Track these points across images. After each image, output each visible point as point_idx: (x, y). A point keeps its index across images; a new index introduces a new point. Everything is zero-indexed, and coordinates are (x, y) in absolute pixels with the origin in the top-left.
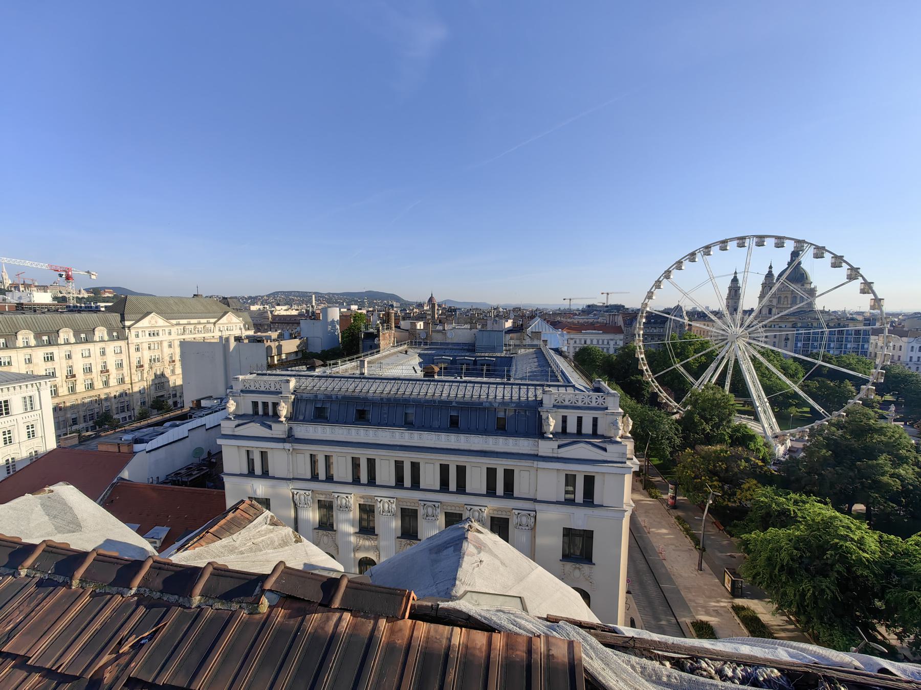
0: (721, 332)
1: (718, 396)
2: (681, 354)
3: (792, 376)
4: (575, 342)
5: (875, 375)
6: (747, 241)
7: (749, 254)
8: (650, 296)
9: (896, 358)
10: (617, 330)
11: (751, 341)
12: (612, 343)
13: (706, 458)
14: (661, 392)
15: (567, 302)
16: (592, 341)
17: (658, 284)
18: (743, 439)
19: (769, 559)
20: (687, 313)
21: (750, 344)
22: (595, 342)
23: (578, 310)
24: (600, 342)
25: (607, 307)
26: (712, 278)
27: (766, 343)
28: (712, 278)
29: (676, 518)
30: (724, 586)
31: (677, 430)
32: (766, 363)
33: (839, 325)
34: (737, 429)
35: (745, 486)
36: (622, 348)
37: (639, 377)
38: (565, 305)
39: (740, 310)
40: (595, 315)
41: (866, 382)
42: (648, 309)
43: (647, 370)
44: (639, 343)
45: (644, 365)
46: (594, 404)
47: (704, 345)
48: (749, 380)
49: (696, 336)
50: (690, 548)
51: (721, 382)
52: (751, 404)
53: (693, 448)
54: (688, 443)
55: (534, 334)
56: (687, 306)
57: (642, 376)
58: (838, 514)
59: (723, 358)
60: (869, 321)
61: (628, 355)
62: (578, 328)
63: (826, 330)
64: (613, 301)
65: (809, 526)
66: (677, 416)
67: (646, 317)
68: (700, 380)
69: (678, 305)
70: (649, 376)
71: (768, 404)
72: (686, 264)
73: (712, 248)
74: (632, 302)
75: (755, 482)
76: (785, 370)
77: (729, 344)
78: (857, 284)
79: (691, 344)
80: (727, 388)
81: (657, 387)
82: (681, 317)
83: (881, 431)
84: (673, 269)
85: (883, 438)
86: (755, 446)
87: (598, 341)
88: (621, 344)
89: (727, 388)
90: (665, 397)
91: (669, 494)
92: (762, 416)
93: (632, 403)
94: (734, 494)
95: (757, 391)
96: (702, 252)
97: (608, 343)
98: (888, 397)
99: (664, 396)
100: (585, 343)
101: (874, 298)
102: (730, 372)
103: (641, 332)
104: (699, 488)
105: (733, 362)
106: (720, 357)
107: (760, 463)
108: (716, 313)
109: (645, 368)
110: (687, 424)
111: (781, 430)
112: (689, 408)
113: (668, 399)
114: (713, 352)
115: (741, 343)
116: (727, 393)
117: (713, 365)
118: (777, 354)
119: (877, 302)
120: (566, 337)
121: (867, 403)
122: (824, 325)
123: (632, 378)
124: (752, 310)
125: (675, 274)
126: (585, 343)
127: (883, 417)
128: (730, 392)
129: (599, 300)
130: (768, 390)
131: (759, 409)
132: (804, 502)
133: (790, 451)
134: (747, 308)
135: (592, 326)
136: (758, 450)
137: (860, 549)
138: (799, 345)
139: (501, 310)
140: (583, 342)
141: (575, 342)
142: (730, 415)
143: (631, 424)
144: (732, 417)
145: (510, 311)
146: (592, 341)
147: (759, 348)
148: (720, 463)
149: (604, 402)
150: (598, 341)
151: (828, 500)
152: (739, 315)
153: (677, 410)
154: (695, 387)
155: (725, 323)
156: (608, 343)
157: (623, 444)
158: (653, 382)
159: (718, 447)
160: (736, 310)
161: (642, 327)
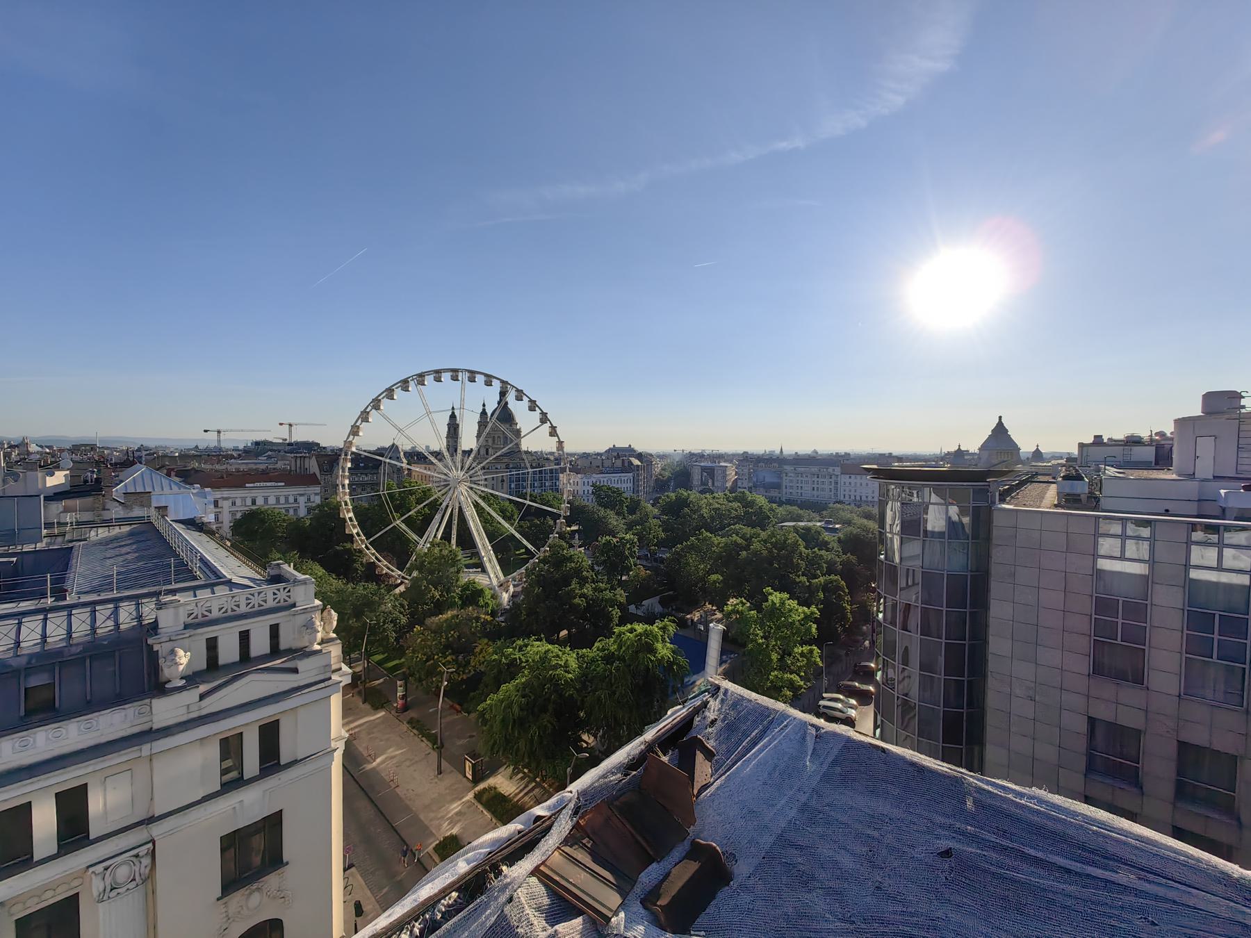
0: (443, 477)
1: (445, 552)
2: (402, 508)
3: (508, 519)
4: (234, 504)
5: (564, 510)
6: (460, 374)
7: (463, 389)
8: (355, 431)
10: (310, 480)
11: (473, 486)
12: (302, 500)
13: (437, 631)
14: (379, 561)
15: (212, 436)
16: (266, 499)
17: (364, 416)
18: (473, 595)
19: (503, 720)
20: (405, 453)
21: (471, 488)
22: (272, 500)
23: (236, 449)
24: (282, 500)
25: (290, 444)
26: (429, 413)
27: (486, 486)
28: (429, 413)
29: (408, 723)
30: (465, 776)
31: (402, 606)
32: (488, 509)
33: (539, 466)
34: (466, 587)
35: (478, 650)
36: (318, 506)
37: (348, 545)
38: (210, 440)
39: (459, 451)
40: (269, 457)
42: (354, 449)
43: (358, 534)
45: (354, 527)
47: (426, 493)
48: (473, 529)
49: (417, 483)
50: (427, 752)
51: (447, 536)
53: (421, 623)
54: (417, 618)
55: (133, 497)
56: (405, 446)
57: (352, 542)
58: (550, 647)
59: (447, 506)
60: (558, 461)
62: (237, 480)
63: (530, 470)
64: (300, 436)
65: (531, 668)
66: (402, 588)
67: (352, 461)
68: (425, 537)
69: (393, 444)
70: (361, 542)
71: (492, 552)
72: (398, 393)
73: (426, 377)
74: (331, 438)
75: (486, 641)
76: (503, 512)
77: (451, 492)
79: (411, 493)
80: (454, 541)
81: (373, 554)
82: (398, 459)
83: (570, 559)
84: (383, 398)
85: (573, 565)
86: (484, 601)
87: (278, 499)
88: (317, 500)
89: (454, 541)
90: (385, 566)
91: (398, 694)
92: (488, 565)
93: (336, 583)
94: (468, 663)
95: (481, 539)
96: (415, 380)
97: (296, 500)
98: (575, 528)
99: (384, 566)
100: (254, 502)
103: (347, 482)
104: (433, 672)
105: (457, 510)
106: (444, 504)
107: (489, 618)
108: (438, 455)
109: (355, 531)
110: (414, 596)
111: (505, 576)
112: (415, 574)
113: (388, 568)
114: (436, 500)
115: (463, 488)
116: (454, 547)
117: (438, 517)
119: (560, 443)
120: (211, 498)
121: (562, 536)
122: (528, 465)
123: (338, 548)
124: (472, 449)
125: (385, 404)
126: (254, 502)
127: (571, 546)
128: (457, 546)
129: (276, 435)
131: (485, 559)
132: (526, 646)
133: (514, 596)
134: (467, 449)
135: (264, 476)
136: (487, 605)
137: (566, 671)
138: (513, 486)
139: (33, 448)
140: (249, 502)
141: (234, 504)
142: (458, 572)
143: (336, 618)
144: (461, 575)
145: (61, 451)
146: (266, 499)
147: (480, 493)
148: (452, 632)
149: (289, 597)
151: (542, 636)
152: (459, 457)
153: (400, 579)
154: (419, 547)
155: (446, 466)
156: (296, 500)
157: (324, 651)
158: (368, 549)
159: (450, 614)
160: (456, 451)
161: (347, 474)
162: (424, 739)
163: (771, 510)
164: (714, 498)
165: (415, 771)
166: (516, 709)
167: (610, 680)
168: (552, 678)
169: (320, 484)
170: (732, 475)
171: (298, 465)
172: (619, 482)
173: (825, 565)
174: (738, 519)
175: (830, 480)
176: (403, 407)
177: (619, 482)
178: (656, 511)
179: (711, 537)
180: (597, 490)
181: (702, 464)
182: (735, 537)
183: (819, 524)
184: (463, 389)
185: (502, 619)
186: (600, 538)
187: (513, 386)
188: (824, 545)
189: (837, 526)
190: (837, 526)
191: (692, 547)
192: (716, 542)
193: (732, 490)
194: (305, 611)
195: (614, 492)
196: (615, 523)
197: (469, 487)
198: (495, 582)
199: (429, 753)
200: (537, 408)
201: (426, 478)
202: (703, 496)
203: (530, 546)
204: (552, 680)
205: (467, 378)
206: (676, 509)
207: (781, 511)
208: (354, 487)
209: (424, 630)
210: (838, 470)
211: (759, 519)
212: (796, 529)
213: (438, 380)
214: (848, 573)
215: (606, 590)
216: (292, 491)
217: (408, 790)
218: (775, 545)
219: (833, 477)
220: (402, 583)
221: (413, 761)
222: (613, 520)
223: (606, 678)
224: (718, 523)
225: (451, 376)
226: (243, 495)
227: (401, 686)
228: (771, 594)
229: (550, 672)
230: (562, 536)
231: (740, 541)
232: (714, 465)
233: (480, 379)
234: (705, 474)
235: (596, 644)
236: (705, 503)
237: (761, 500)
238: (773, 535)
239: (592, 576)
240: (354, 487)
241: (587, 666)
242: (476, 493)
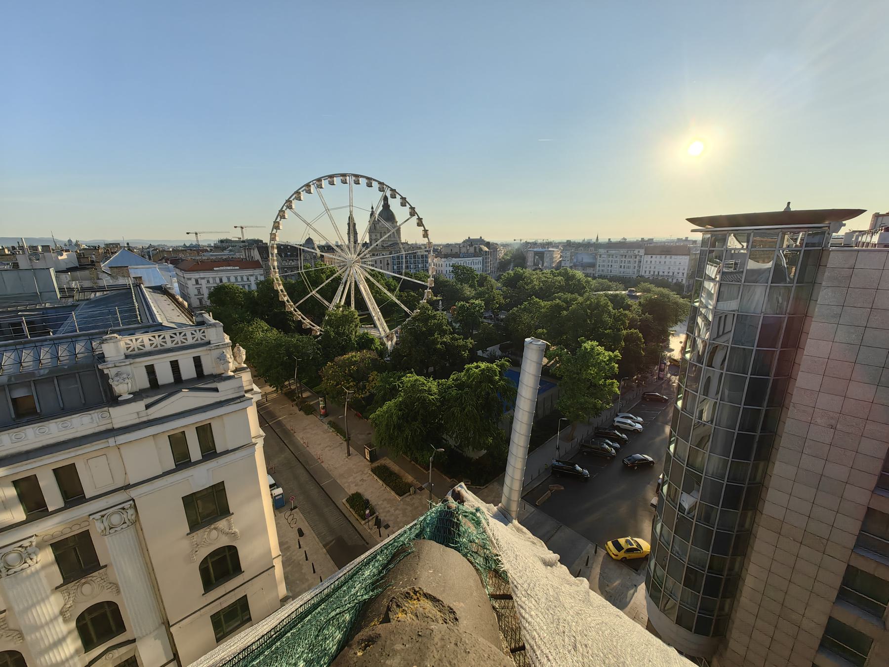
4: (208, 282)
5: (430, 283)
7: (351, 190)
8: (276, 226)
9: (441, 272)
14: (304, 320)
17: (281, 215)
19: (387, 425)
28: (327, 210)
29: (328, 424)
30: (365, 458)
32: (375, 282)
41: (425, 287)
43: (288, 301)
44: (276, 275)
46: (190, 341)
47: (333, 272)
48: (366, 297)
51: (348, 302)
52: (370, 315)
55: (115, 270)
61: (267, 286)
71: (380, 313)
77: (349, 269)
78: (414, 219)
79: (322, 271)
80: (353, 305)
81: (300, 315)
83: (434, 317)
84: (293, 200)
87: (236, 278)
89: (353, 305)
91: (321, 406)
92: (377, 323)
95: (372, 304)
96: (315, 185)
97: (248, 279)
99: (307, 322)
102: (353, 292)
105: (353, 283)
106: (344, 281)
109: (285, 299)
117: (341, 288)
118: (382, 274)
119: (426, 234)
121: (430, 302)
125: (295, 204)
130: (379, 302)
131: (375, 318)
137: (429, 394)
138: (395, 267)
141: (208, 282)
143: (244, 353)
147: (369, 270)
148: (353, 367)
149: (205, 336)
150: (236, 278)
151: (413, 370)
156: (248, 279)
157: (236, 376)
158: (296, 311)
162: (338, 434)
163: (588, 282)
165: (333, 453)
166: (394, 417)
167: (461, 400)
168: (419, 399)
169: (263, 268)
170: (557, 256)
171: (247, 255)
172: (472, 264)
173: (627, 322)
174: (561, 289)
175: (635, 260)
176: (308, 205)
177: (472, 264)
178: (499, 285)
180: (456, 268)
181: (535, 250)
182: (558, 301)
183: (624, 292)
184: (351, 190)
185: (388, 359)
186: (457, 304)
187: (389, 187)
188: (628, 307)
189: (638, 294)
190: (638, 294)
191: (525, 310)
193: (557, 268)
194: (218, 347)
196: (468, 293)
197: (360, 267)
198: (383, 334)
199: (342, 443)
200: (407, 204)
201: (331, 261)
202: (534, 272)
203: (406, 309)
204: (419, 400)
205: (353, 181)
206: (513, 283)
207: (594, 283)
208: (285, 269)
209: (334, 365)
210: (642, 252)
211: (578, 288)
212: (606, 295)
213: (332, 183)
214: (644, 327)
215: (460, 339)
216: (246, 273)
217: (329, 465)
218: (589, 307)
219: (638, 257)
220: (320, 334)
221: (332, 447)
222: (468, 291)
223: (458, 399)
224: (545, 292)
225: (341, 180)
226: (214, 276)
227: (321, 401)
228: (585, 342)
229: (418, 395)
230: (430, 302)
231: (561, 303)
232: (544, 250)
233: (363, 181)
234: (537, 257)
235: (451, 377)
236: (534, 277)
237: (579, 274)
238: (588, 299)
239: (450, 329)
240: (285, 269)
241: (444, 391)
242: (366, 271)
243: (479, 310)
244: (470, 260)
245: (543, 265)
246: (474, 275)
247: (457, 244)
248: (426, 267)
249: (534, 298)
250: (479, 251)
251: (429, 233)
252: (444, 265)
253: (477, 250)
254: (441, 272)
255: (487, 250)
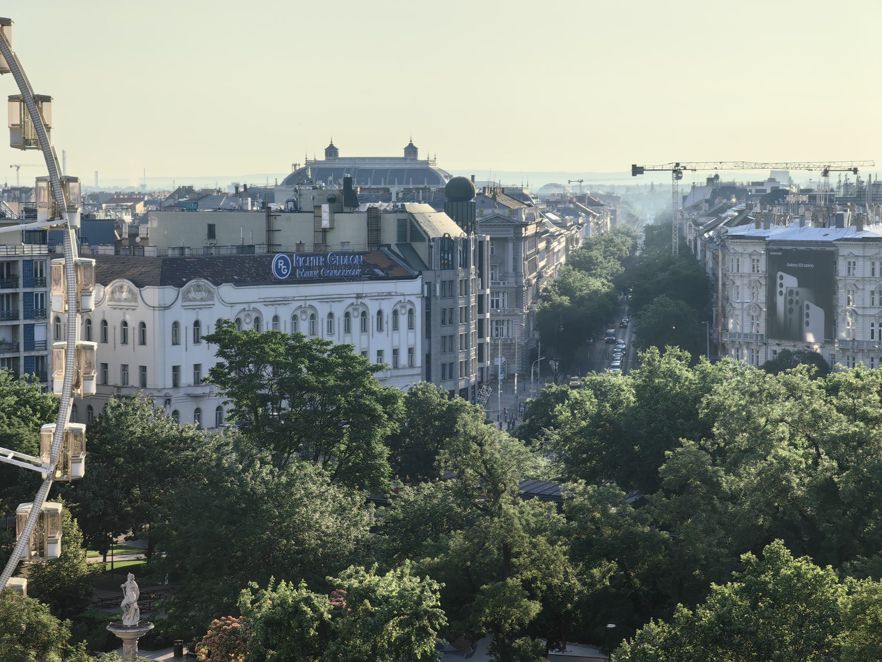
9: (134, 379)
101: (17, 92)
164: (833, 390)
172: (356, 323)
177: (356, 323)
179: (819, 581)
181: (776, 232)
186: (246, 597)
192: (843, 600)
195: (327, 367)
196: (330, 523)
202: (773, 382)
232: (832, 234)
234: (790, 282)
243: (404, 640)
244: (339, 299)
245: (830, 333)
246: (368, 401)
247: (250, 192)
248: (30, 343)
249: (786, 552)
250: (401, 235)
251: (53, 114)
252: (157, 331)
253: (390, 235)
254: (134, 379)
255: (455, 230)
